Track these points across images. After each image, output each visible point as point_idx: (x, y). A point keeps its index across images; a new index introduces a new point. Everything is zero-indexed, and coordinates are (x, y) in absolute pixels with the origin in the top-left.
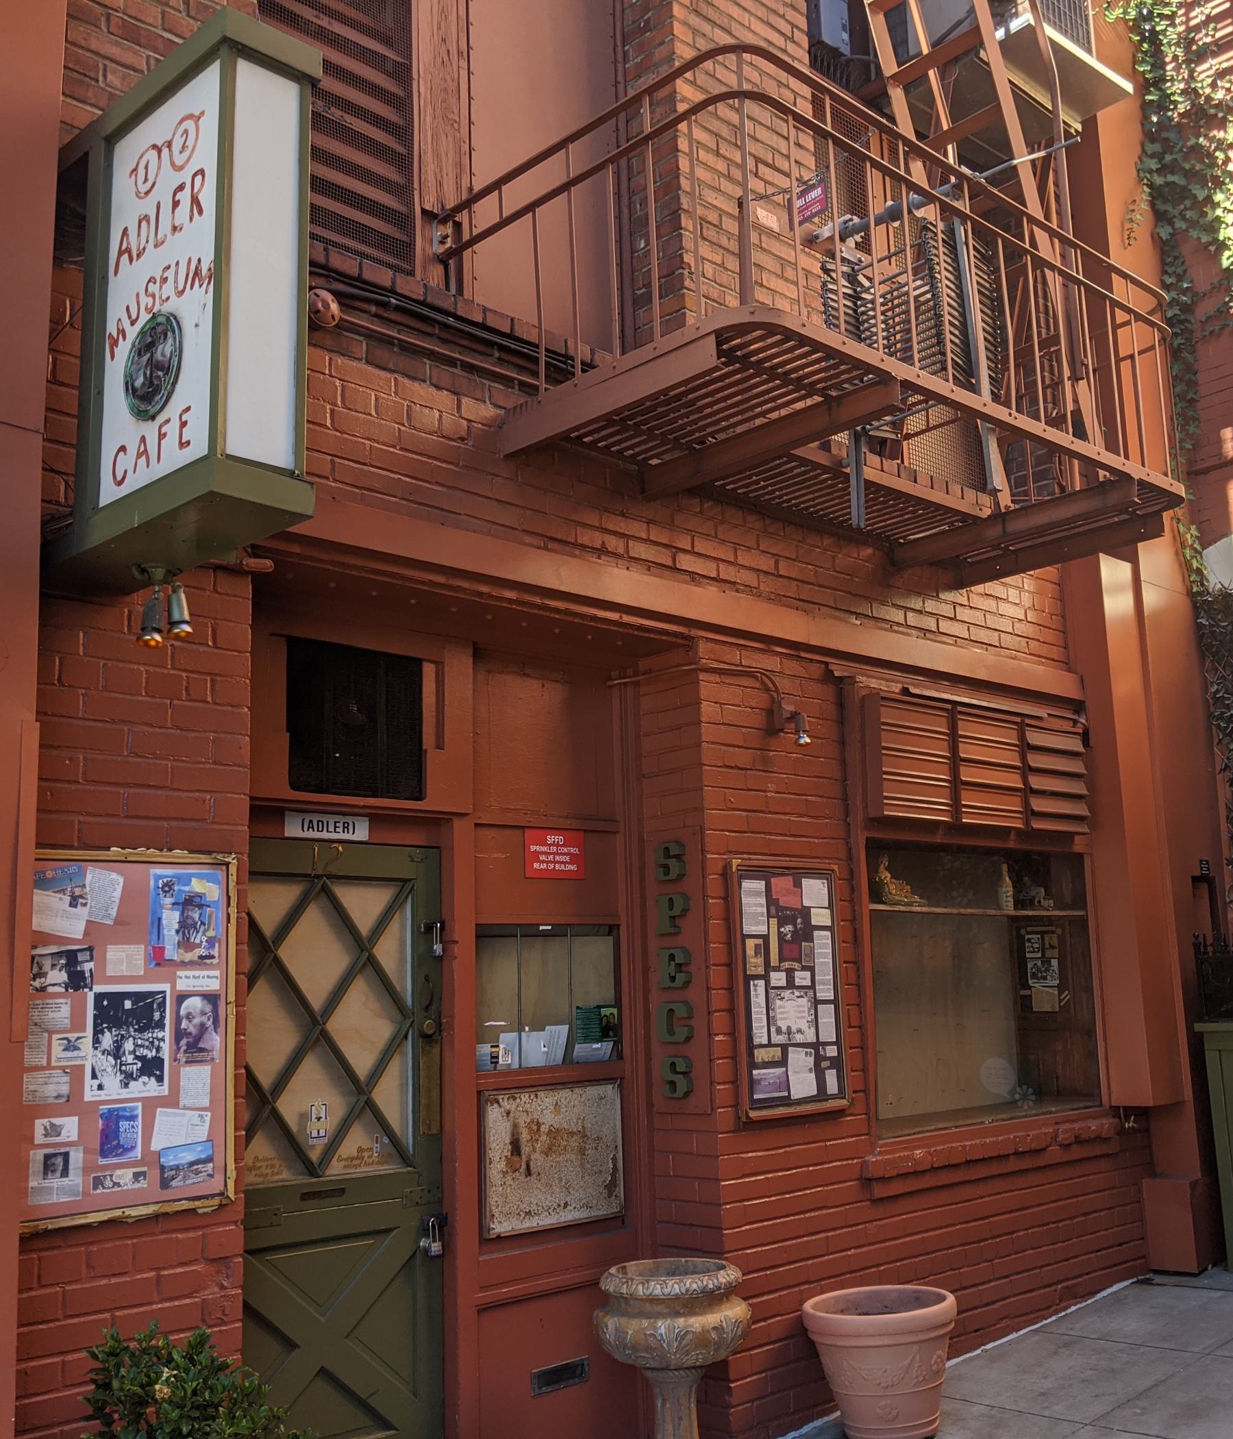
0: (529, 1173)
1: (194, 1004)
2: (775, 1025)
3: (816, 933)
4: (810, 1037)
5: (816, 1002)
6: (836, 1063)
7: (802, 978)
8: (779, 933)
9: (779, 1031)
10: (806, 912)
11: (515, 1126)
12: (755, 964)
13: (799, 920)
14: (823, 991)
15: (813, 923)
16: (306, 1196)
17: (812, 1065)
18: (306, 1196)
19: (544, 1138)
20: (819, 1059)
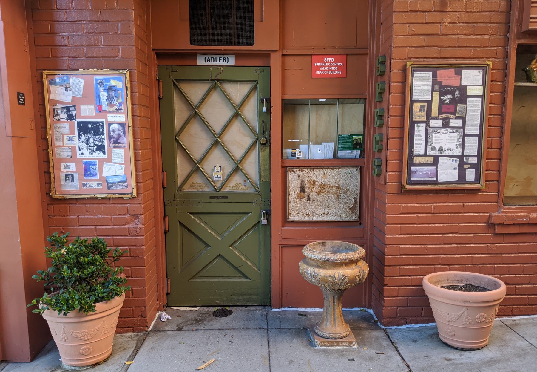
0: (309, 199)
1: (115, 126)
3: (469, 99)
5: (464, 135)
9: (433, 149)
10: (463, 89)
11: (302, 181)
12: (419, 114)
13: (457, 93)
16: (211, 197)
18: (211, 197)
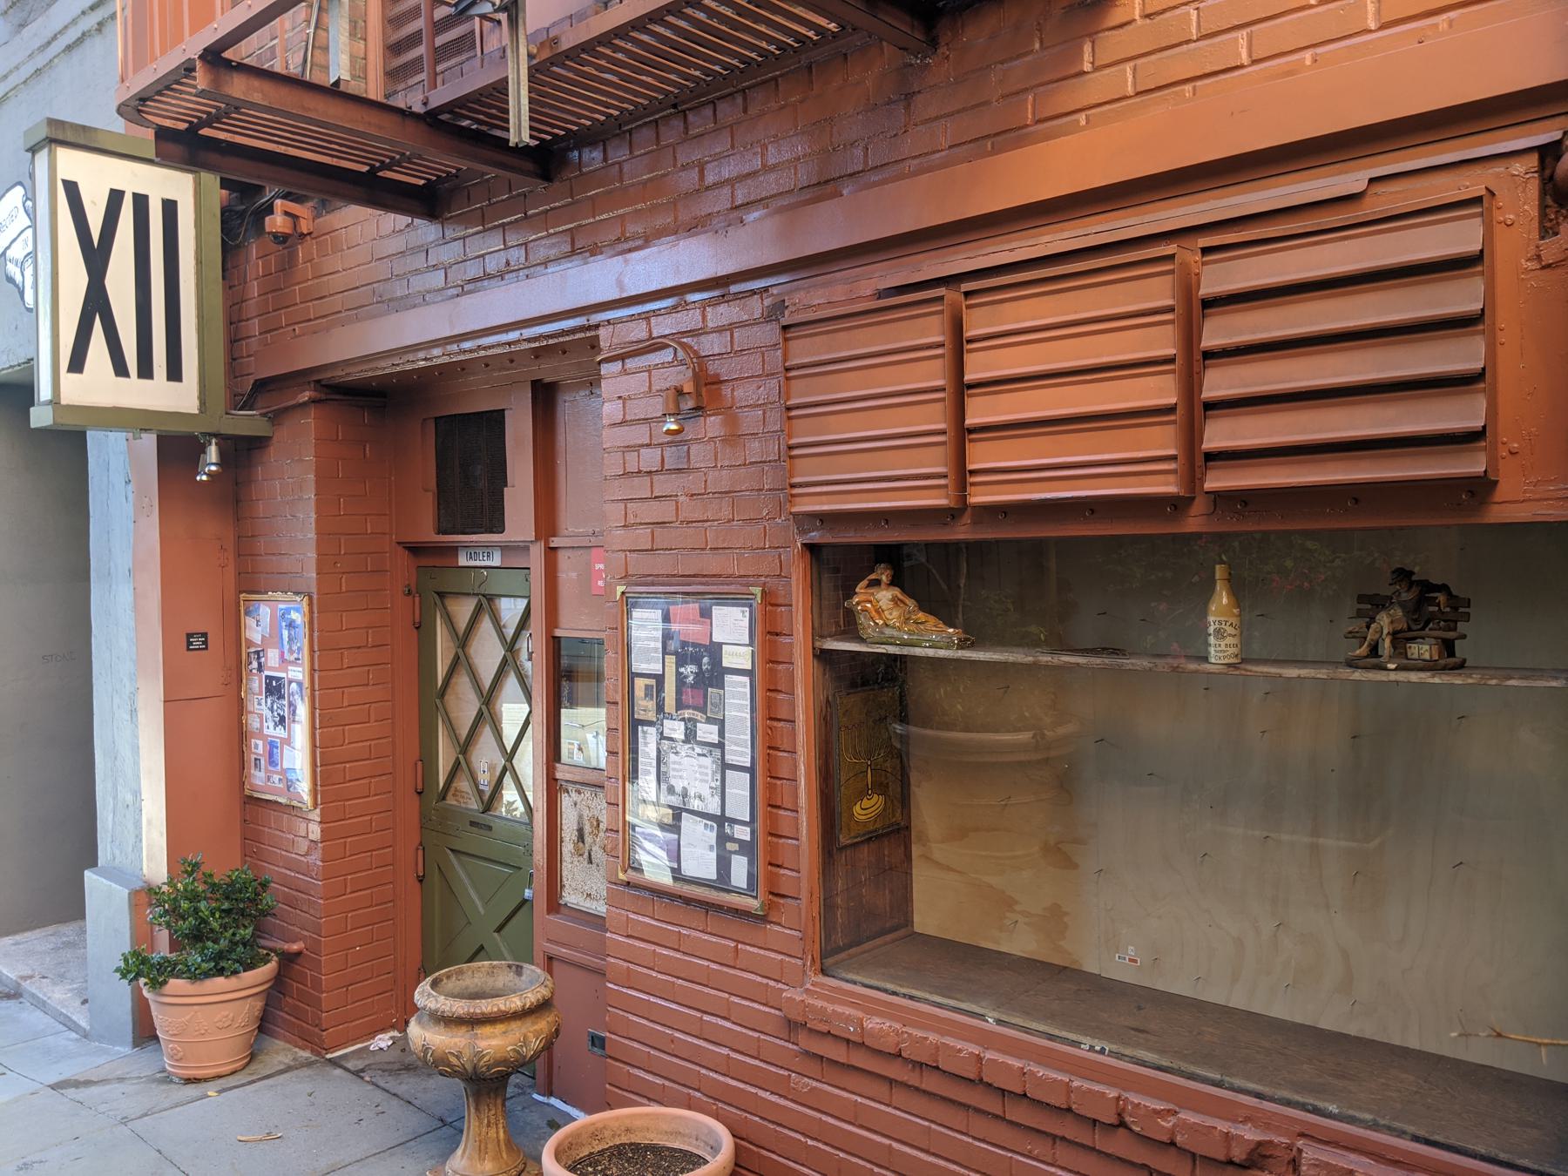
0: (590, 862)
1: (294, 685)
2: (666, 781)
3: (728, 678)
4: (713, 807)
5: (725, 766)
6: (746, 848)
7: (707, 732)
8: (678, 674)
9: (671, 790)
10: (715, 650)
11: (581, 817)
12: (645, 707)
13: (705, 660)
14: (735, 753)
15: (725, 663)
16: (473, 824)
17: (714, 842)
18: (473, 824)
19: (602, 834)
20: (723, 839)
